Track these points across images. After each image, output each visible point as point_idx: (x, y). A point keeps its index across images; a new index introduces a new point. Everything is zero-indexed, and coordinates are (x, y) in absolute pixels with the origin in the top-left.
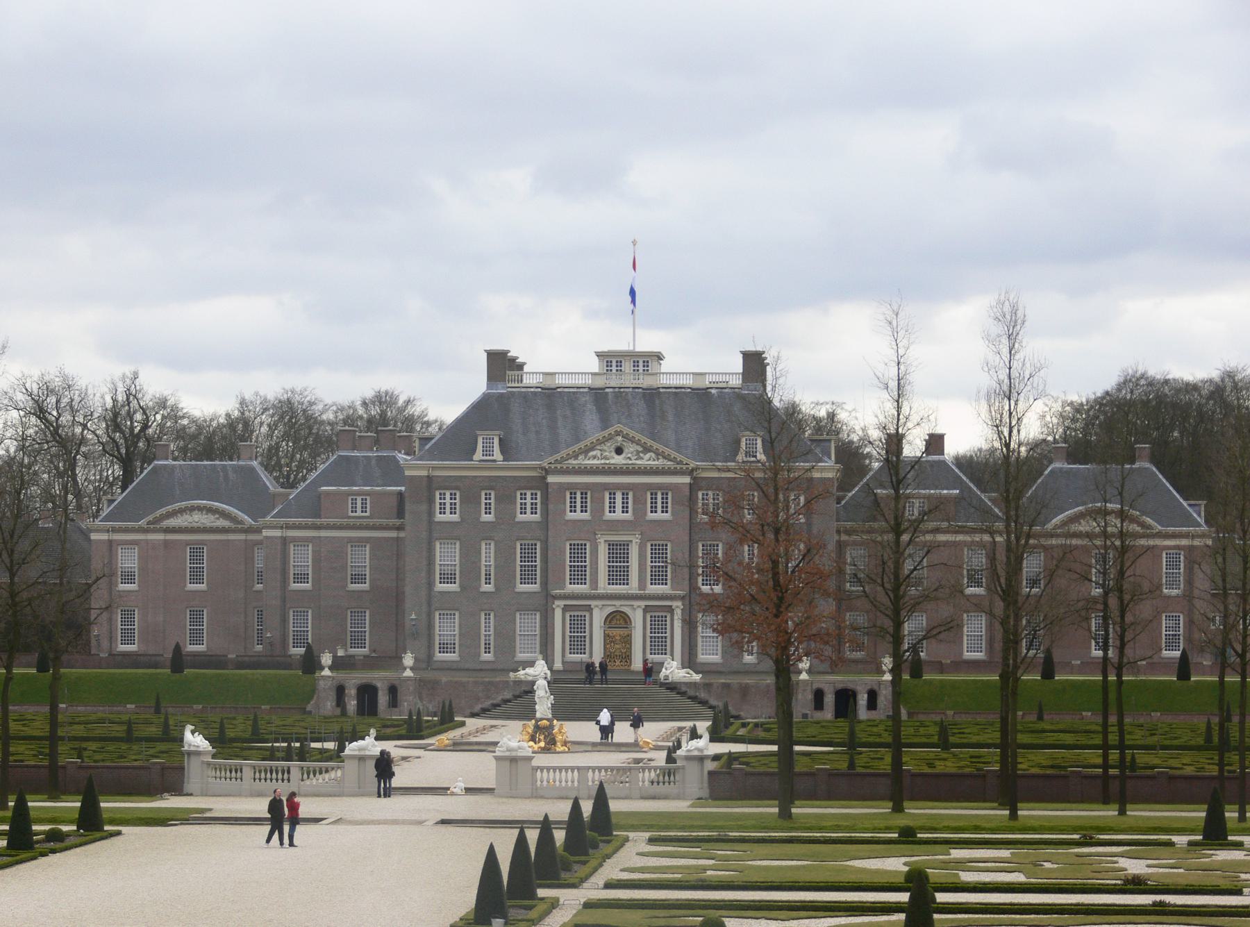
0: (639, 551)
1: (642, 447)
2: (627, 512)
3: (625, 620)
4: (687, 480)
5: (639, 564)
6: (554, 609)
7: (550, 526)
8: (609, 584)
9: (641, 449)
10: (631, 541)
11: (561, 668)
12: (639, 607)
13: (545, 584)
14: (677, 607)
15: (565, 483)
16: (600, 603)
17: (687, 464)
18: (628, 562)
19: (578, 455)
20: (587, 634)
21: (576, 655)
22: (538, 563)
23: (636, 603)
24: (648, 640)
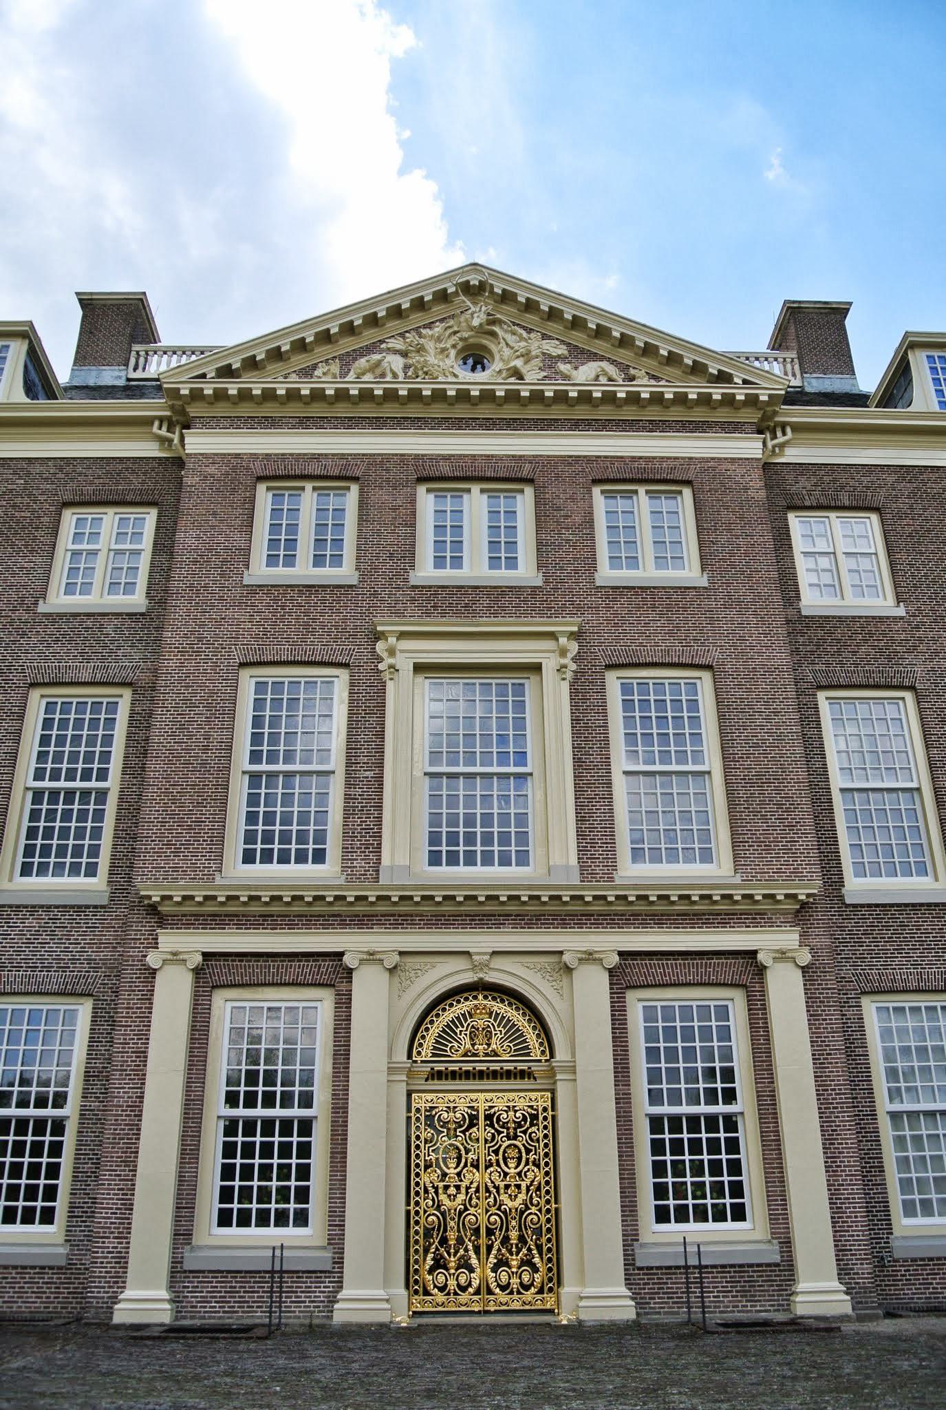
0: (575, 707)
1: (562, 342)
2: (512, 563)
3: (514, 1034)
4: (750, 447)
5: (578, 762)
6: (153, 972)
7: (179, 611)
8: (435, 859)
9: (562, 350)
10: (537, 668)
11: (162, 1314)
12: (589, 957)
13: (123, 868)
14: (782, 956)
15: (254, 456)
16: (388, 941)
17: (745, 382)
18: (521, 758)
19: (315, 367)
20: (320, 1110)
21: (253, 1231)
22: (113, 783)
23: (572, 942)
24: (643, 1137)
